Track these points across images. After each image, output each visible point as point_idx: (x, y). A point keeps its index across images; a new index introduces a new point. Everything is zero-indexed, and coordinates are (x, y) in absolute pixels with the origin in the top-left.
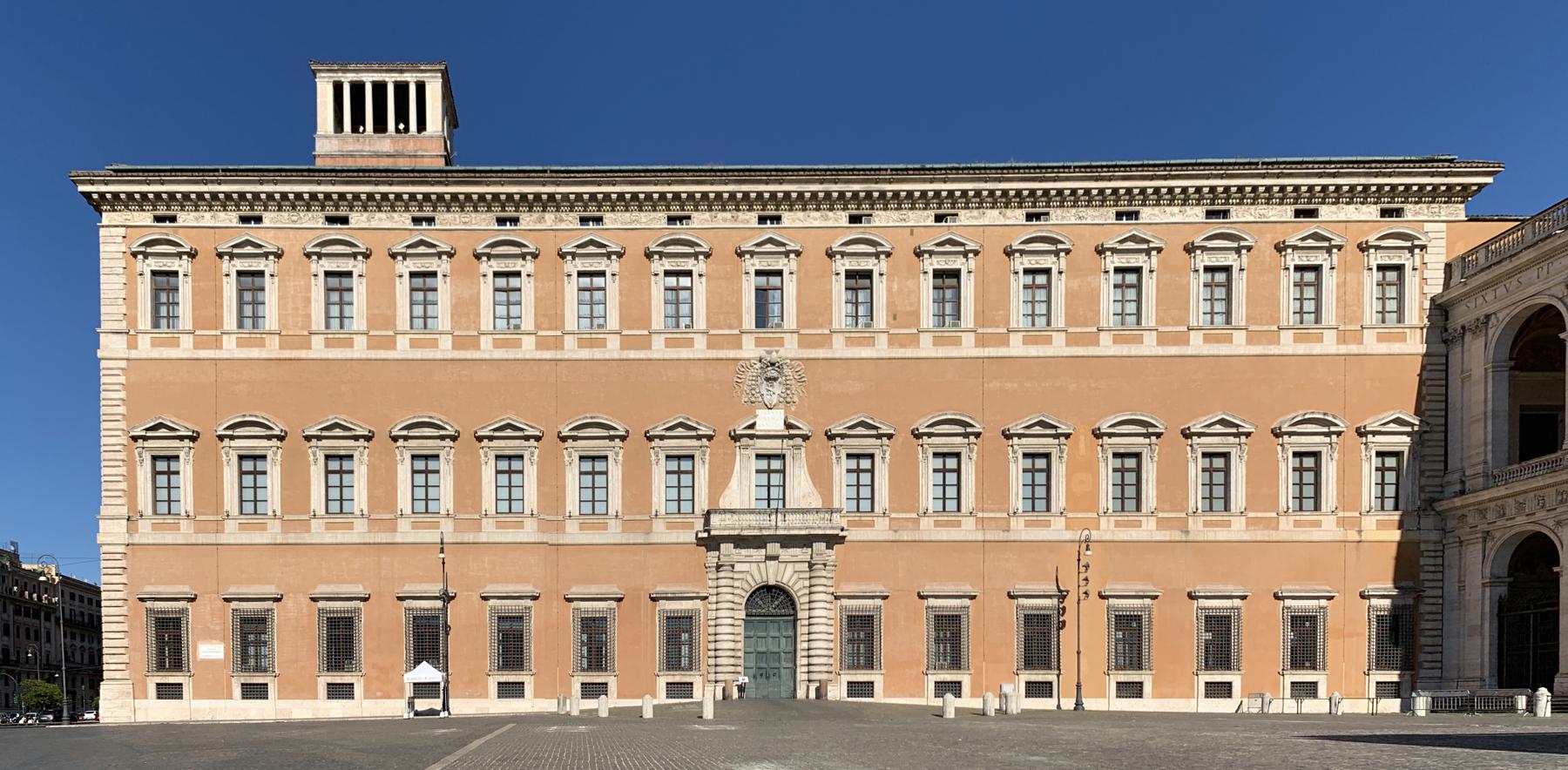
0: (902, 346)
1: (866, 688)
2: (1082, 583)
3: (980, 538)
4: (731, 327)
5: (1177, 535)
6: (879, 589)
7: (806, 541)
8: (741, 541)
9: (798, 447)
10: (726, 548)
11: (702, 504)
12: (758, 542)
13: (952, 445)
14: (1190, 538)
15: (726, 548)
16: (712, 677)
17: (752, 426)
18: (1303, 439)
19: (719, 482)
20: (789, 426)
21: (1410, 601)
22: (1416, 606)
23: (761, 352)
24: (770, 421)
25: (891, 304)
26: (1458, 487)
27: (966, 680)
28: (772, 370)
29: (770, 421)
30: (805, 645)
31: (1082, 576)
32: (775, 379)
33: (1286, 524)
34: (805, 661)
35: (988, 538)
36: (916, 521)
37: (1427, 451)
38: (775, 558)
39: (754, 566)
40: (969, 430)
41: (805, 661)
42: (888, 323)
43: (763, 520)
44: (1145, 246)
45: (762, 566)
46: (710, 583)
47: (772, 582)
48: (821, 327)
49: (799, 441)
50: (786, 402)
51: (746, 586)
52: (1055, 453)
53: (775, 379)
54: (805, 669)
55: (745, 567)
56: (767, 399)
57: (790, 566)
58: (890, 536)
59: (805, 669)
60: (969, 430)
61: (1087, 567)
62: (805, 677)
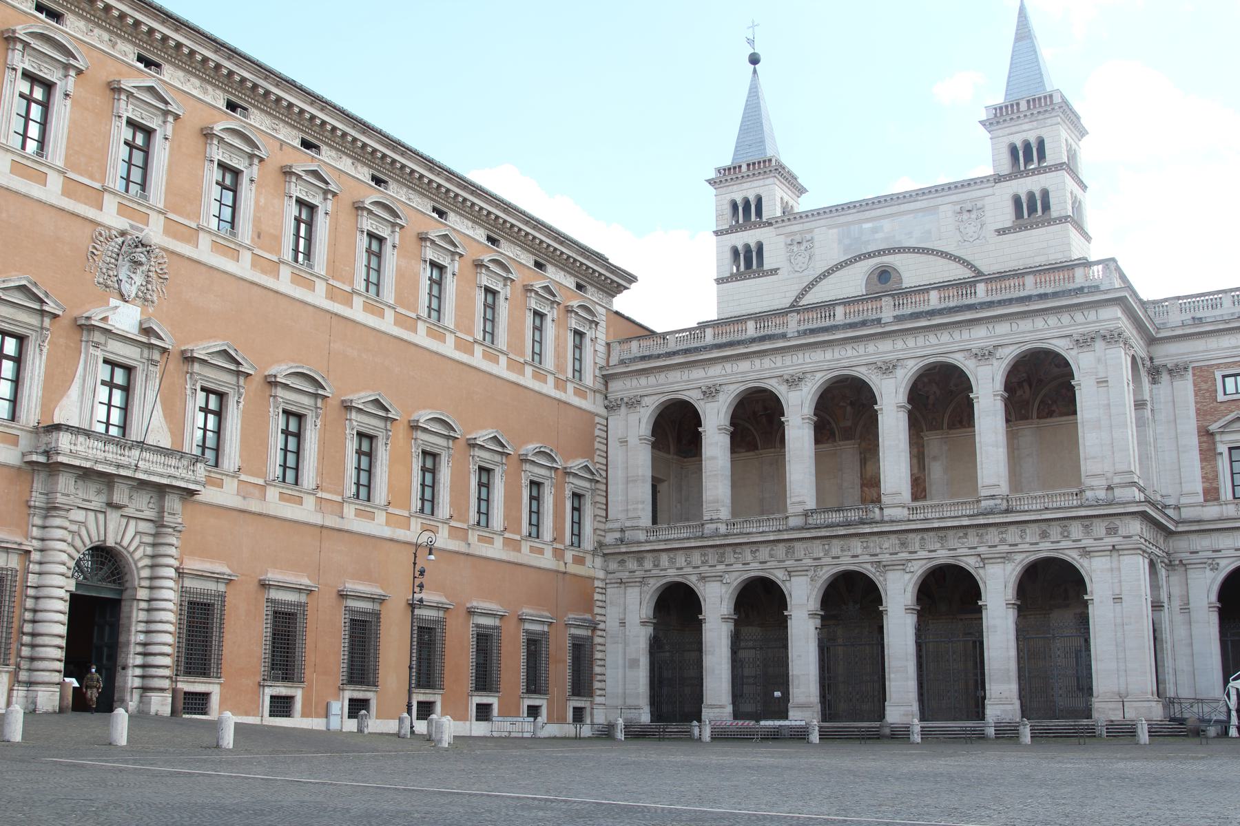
0: (264, 272)
1: (198, 702)
2: (417, 590)
3: (320, 522)
4: (92, 177)
5: (462, 548)
6: (221, 568)
7: (161, 490)
8: (86, 474)
9: (154, 363)
10: (65, 483)
11: (31, 414)
12: (108, 480)
13: (302, 406)
14: (471, 551)
15: (65, 483)
16: (23, 676)
17: (105, 319)
18: (537, 470)
19: (55, 388)
20: (147, 331)
21: (589, 633)
22: (592, 638)
23: (121, 223)
24: (126, 318)
25: (257, 221)
26: (618, 535)
27: (298, 694)
28: (135, 250)
29: (126, 318)
30: (141, 637)
31: (417, 582)
32: (141, 264)
33: (525, 547)
34: (139, 660)
35: (328, 523)
36: (263, 488)
37: (599, 499)
38: (118, 507)
39: (91, 515)
40: (321, 392)
41: (139, 660)
42: (252, 239)
43: (112, 453)
44: (452, 249)
45: (101, 517)
46: (35, 532)
47: (110, 543)
48: (188, 217)
49: (156, 356)
50: (144, 299)
51: (78, 543)
52: (381, 436)
53: (141, 264)
54: (138, 672)
55: (79, 515)
56: (125, 287)
57: (132, 523)
58: (236, 502)
59: (138, 672)
60: (321, 392)
61: (422, 573)
62: (138, 682)
